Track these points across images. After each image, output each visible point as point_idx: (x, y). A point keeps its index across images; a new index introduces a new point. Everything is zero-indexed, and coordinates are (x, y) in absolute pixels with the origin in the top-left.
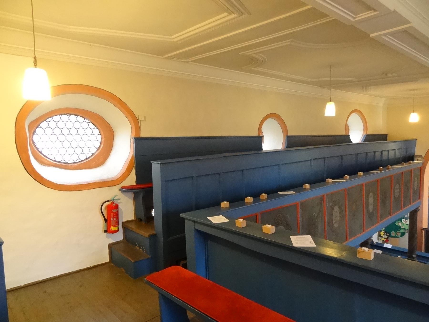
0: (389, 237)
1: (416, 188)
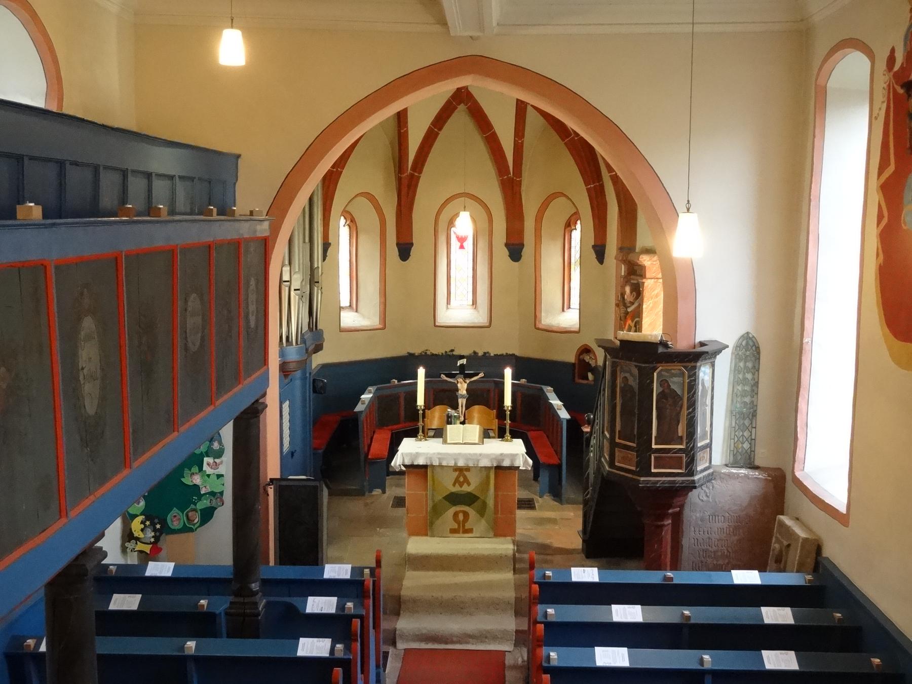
0: (161, 534)
1: (252, 324)
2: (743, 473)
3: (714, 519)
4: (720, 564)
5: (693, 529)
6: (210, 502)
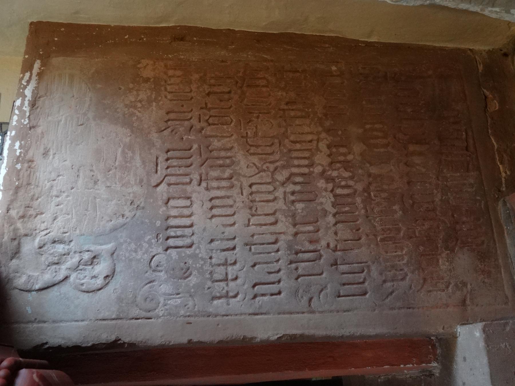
2: (12, 146)
3: (179, 232)
4: (334, 205)
5: (215, 302)
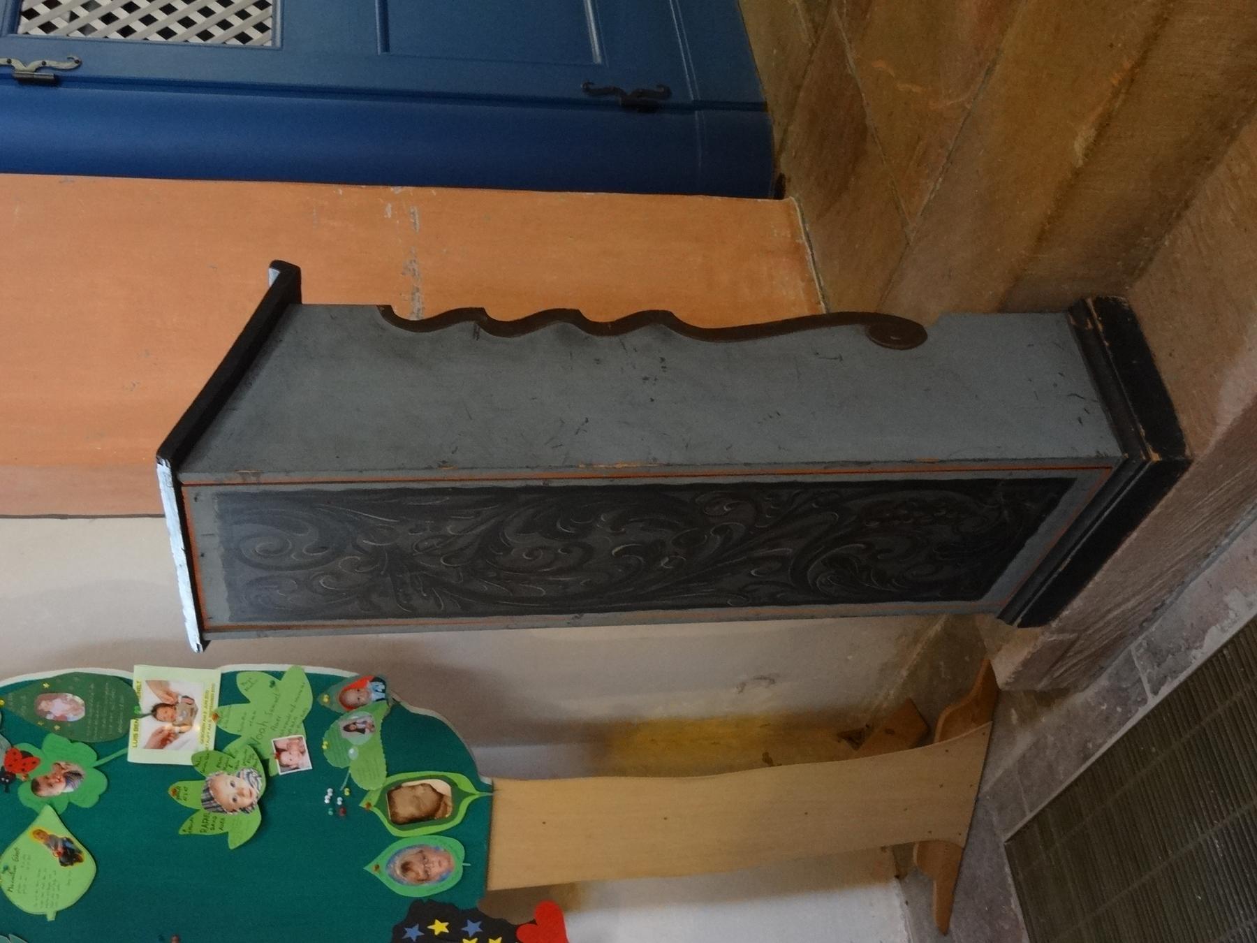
6: (362, 731)
